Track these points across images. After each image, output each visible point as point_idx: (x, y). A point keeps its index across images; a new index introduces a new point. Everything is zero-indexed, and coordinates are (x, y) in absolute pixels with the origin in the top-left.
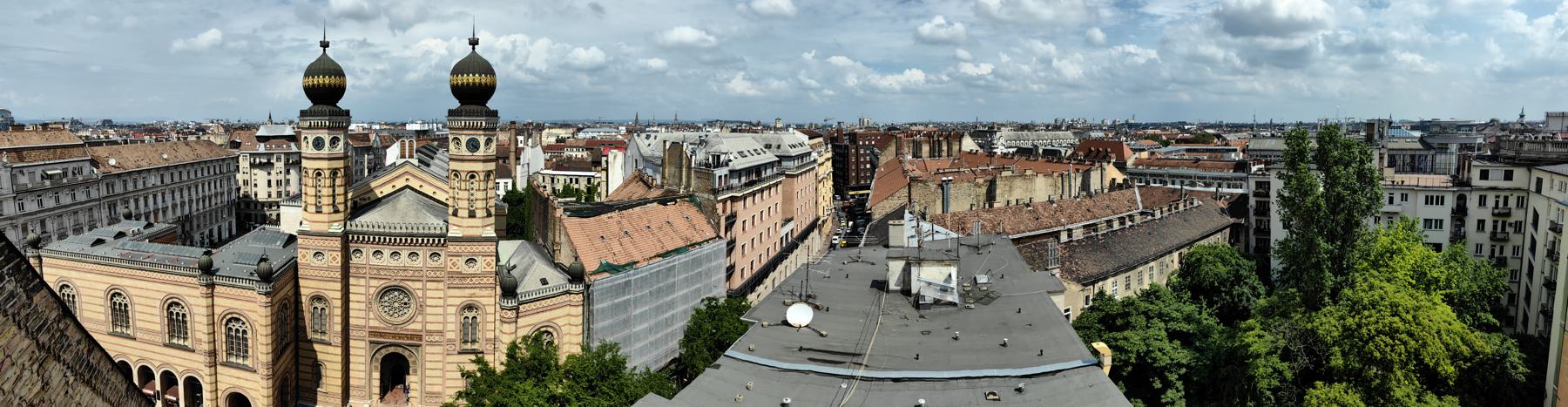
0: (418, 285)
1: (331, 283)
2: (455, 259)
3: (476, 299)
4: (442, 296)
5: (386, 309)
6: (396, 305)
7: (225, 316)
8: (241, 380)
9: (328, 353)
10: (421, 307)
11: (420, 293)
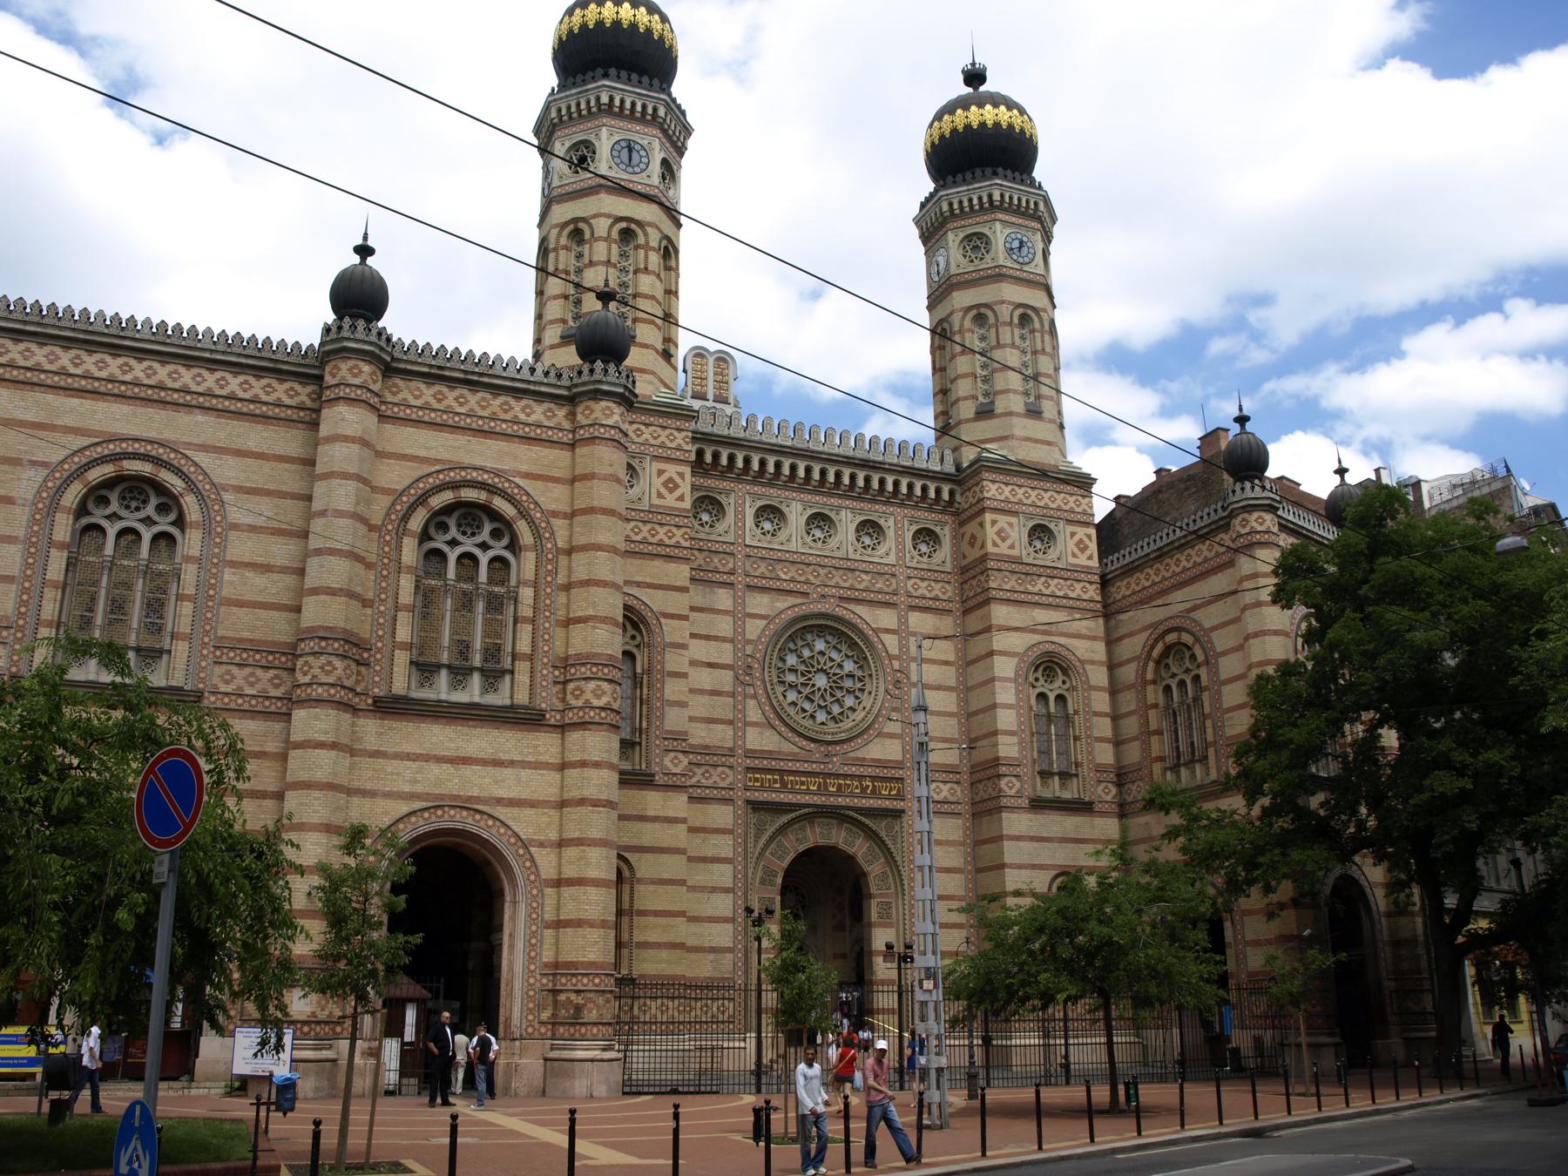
0: (886, 618)
1: (657, 563)
2: (1003, 520)
3: (1062, 640)
4: (951, 657)
5: (792, 696)
6: (821, 681)
7: (422, 500)
8: (467, 771)
9: (642, 818)
11: (891, 642)
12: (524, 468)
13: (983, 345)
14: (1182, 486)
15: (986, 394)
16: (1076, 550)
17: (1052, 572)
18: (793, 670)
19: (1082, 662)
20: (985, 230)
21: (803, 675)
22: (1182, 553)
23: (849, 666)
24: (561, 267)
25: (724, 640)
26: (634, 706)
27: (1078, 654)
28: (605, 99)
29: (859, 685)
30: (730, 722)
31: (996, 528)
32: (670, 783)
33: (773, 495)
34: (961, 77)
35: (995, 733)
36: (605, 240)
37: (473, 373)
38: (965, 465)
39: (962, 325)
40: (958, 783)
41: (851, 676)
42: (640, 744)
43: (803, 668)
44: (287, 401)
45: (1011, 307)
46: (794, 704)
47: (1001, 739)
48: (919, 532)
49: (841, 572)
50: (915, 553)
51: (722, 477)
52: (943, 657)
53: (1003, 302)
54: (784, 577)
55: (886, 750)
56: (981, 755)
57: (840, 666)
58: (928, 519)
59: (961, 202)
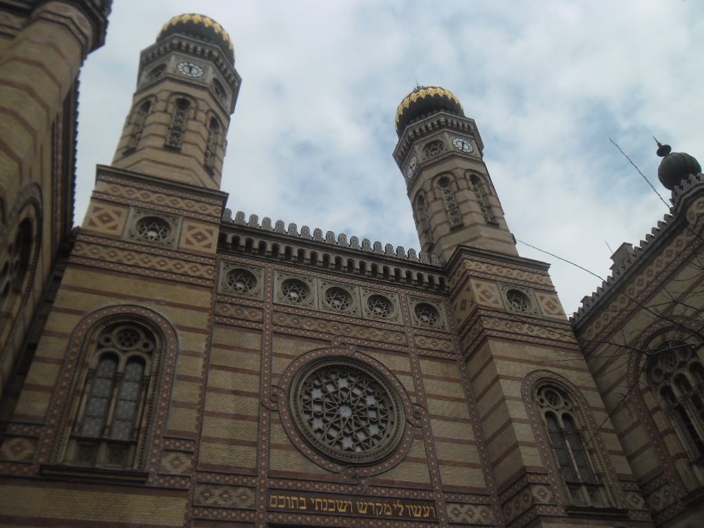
0: (399, 363)
1: (179, 288)
2: (485, 285)
4: (462, 396)
5: (318, 424)
6: (346, 413)
10: (419, 414)
15: (456, 220)
18: (318, 402)
19: (578, 388)
20: (439, 138)
21: (328, 407)
22: (641, 273)
23: (371, 401)
25: (251, 372)
26: (137, 408)
29: (381, 417)
30: (254, 444)
31: (480, 289)
32: (166, 485)
33: (299, 273)
35: (516, 445)
40: (488, 505)
41: (372, 408)
42: (136, 443)
43: (327, 400)
45: (464, 171)
46: (319, 431)
47: (523, 449)
49: (358, 328)
50: (419, 320)
51: (254, 257)
53: (458, 168)
54: (308, 328)
55: (410, 473)
56: (506, 470)
57: (363, 401)
58: (428, 298)
59: (420, 129)
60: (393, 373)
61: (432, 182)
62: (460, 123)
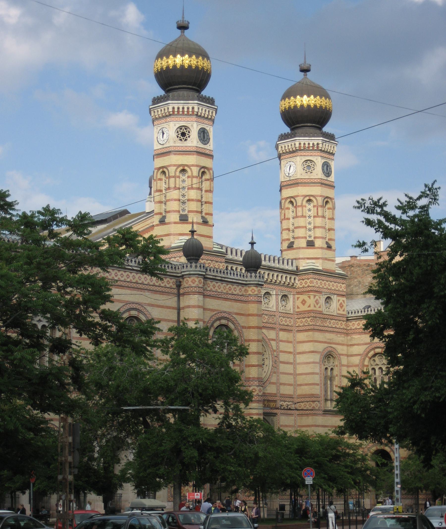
0: (271, 334)
4: (291, 350)
11: (273, 343)
12: (235, 311)
13: (310, 213)
14: (365, 268)
15: (310, 236)
16: (340, 308)
17: (331, 317)
19: (340, 355)
24: (177, 186)
27: (338, 351)
28: (196, 110)
34: (298, 69)
36: (196, 177)
37: (223, 277)
38: (301, 268)
39: (302, 203)
44: (168, 286)
45: (323, 198)
48: (282, 297)
52: (289, 350)
53: (321, 196)
60: (270, 340)
61: (303, 200)
62: (330, 145)
